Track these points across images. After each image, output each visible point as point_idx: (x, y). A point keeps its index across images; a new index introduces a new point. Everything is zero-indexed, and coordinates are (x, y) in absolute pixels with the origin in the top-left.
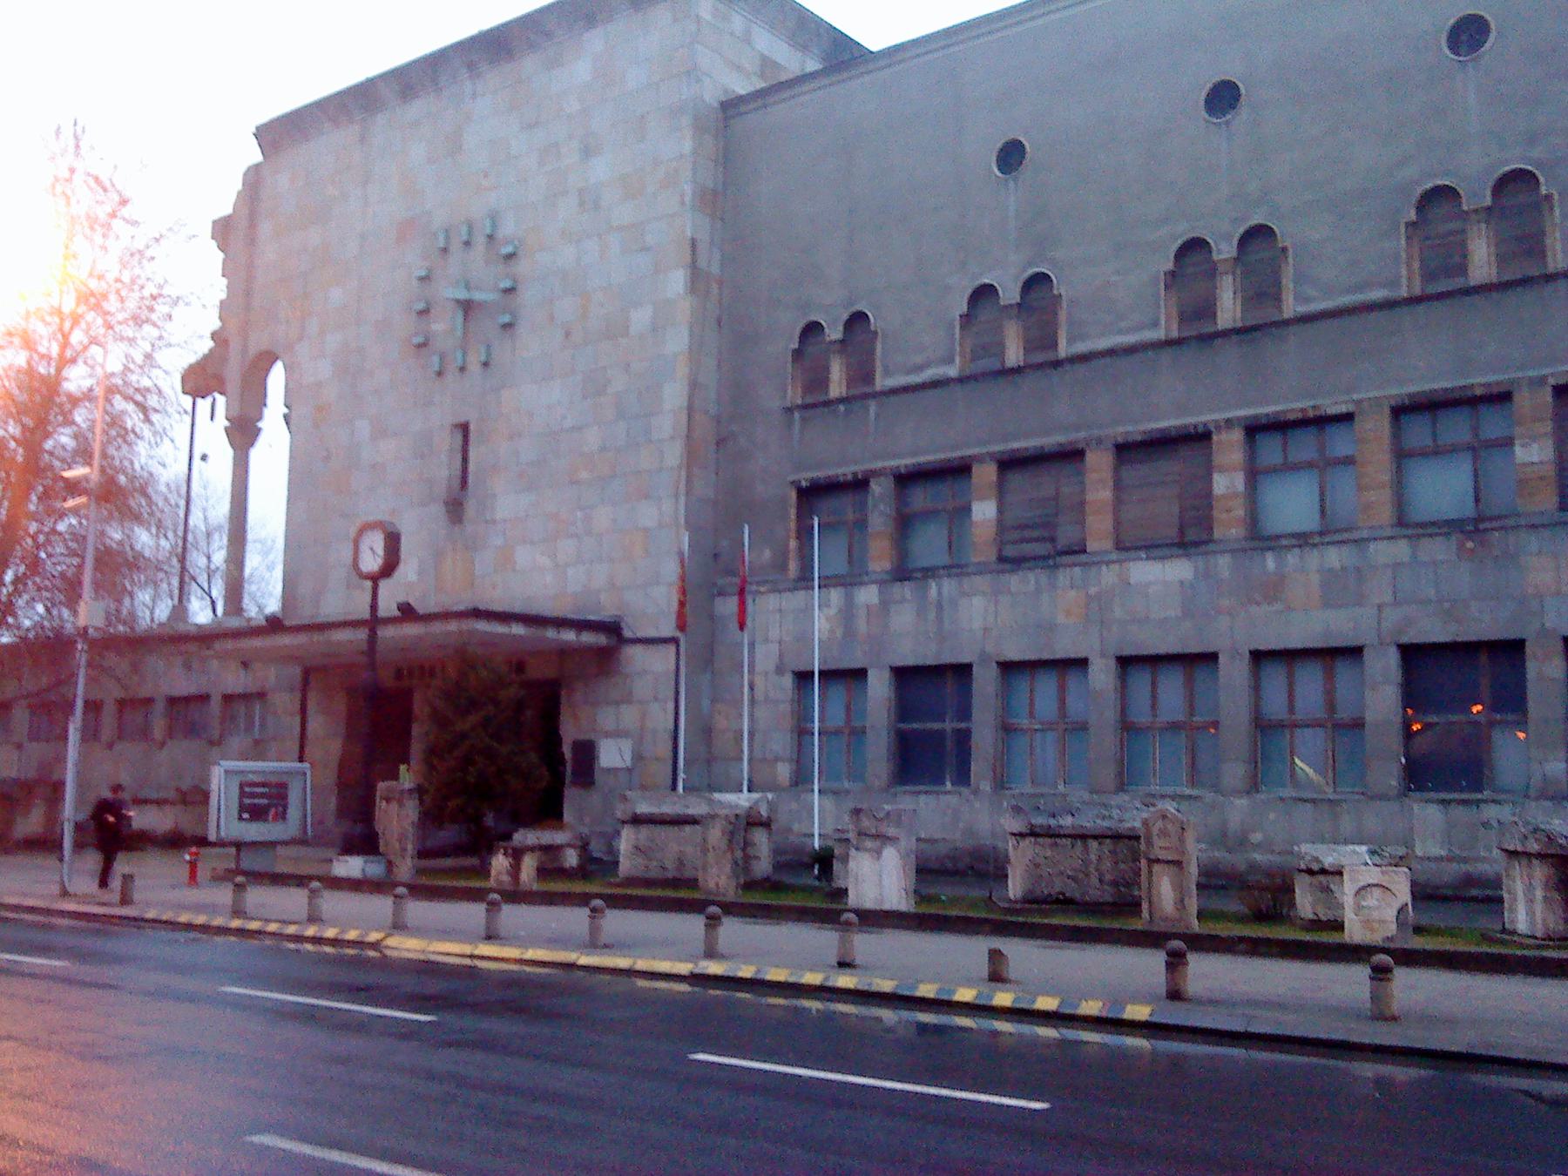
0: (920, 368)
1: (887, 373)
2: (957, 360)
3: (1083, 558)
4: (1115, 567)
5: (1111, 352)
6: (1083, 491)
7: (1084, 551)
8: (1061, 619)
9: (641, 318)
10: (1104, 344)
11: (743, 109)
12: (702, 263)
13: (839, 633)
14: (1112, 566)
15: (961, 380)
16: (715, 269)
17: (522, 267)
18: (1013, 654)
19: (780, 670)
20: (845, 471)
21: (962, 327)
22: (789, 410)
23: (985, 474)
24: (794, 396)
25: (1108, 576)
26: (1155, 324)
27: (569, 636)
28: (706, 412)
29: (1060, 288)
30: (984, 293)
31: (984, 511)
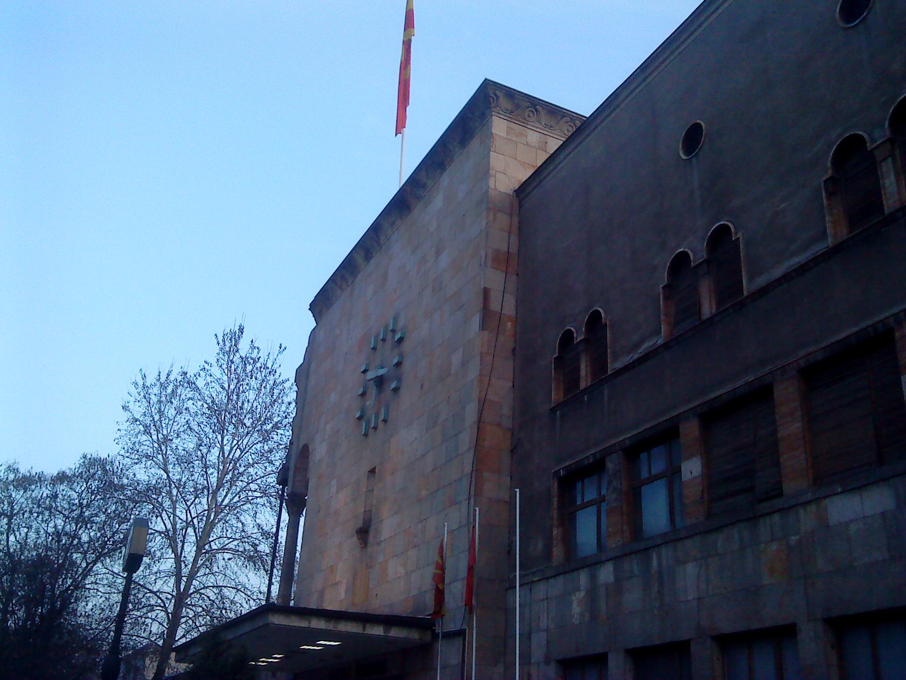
0: (637, 346)
1: (616, 358)
2: (663, 328)
3: (778, 503)
4: (812, 508)
5: (786, 278)
6: (775, 432)
7: (781, 495)
8: (767, 580)
9: (457, 359)
10: (778, 272)
11: (529, 190)
12: (495, 306)
13: (587, 615)
14: (809, 508)
15: (666, 346)
16: (509, 309)
17: (406, 346)
18: (727, 627)
19: (547, 660)
20: (588, 455)
21: (666, 298)
22: (553, 410)
23: (690, 430)
24: (556, 396)
25: (806, 520)
26: (824, 235)
27: (378, 631)
28: (499, 425)
29: (738, 235)
30: (681, 261)
31: (692, 468)
